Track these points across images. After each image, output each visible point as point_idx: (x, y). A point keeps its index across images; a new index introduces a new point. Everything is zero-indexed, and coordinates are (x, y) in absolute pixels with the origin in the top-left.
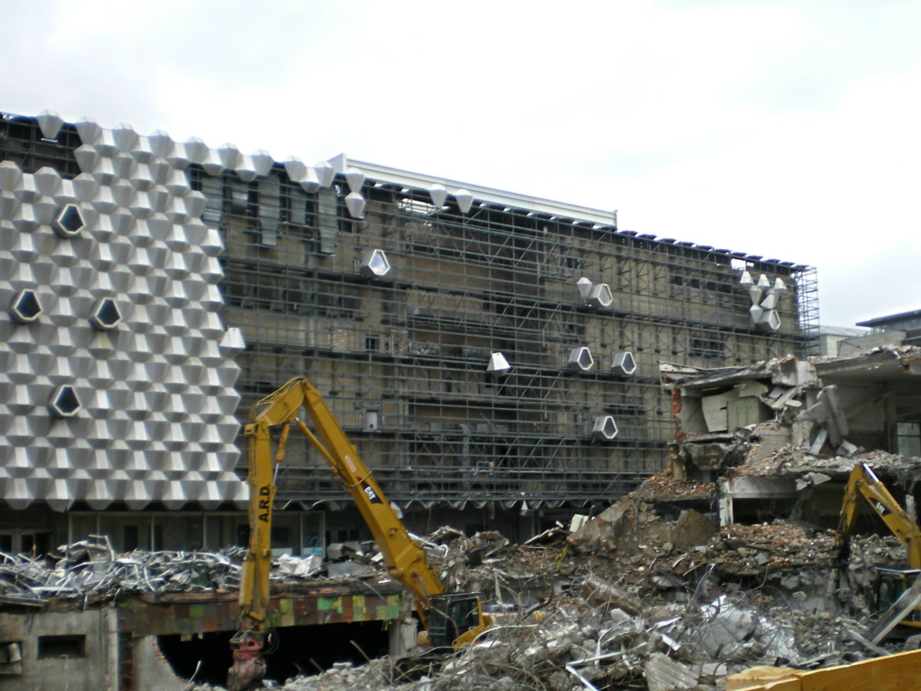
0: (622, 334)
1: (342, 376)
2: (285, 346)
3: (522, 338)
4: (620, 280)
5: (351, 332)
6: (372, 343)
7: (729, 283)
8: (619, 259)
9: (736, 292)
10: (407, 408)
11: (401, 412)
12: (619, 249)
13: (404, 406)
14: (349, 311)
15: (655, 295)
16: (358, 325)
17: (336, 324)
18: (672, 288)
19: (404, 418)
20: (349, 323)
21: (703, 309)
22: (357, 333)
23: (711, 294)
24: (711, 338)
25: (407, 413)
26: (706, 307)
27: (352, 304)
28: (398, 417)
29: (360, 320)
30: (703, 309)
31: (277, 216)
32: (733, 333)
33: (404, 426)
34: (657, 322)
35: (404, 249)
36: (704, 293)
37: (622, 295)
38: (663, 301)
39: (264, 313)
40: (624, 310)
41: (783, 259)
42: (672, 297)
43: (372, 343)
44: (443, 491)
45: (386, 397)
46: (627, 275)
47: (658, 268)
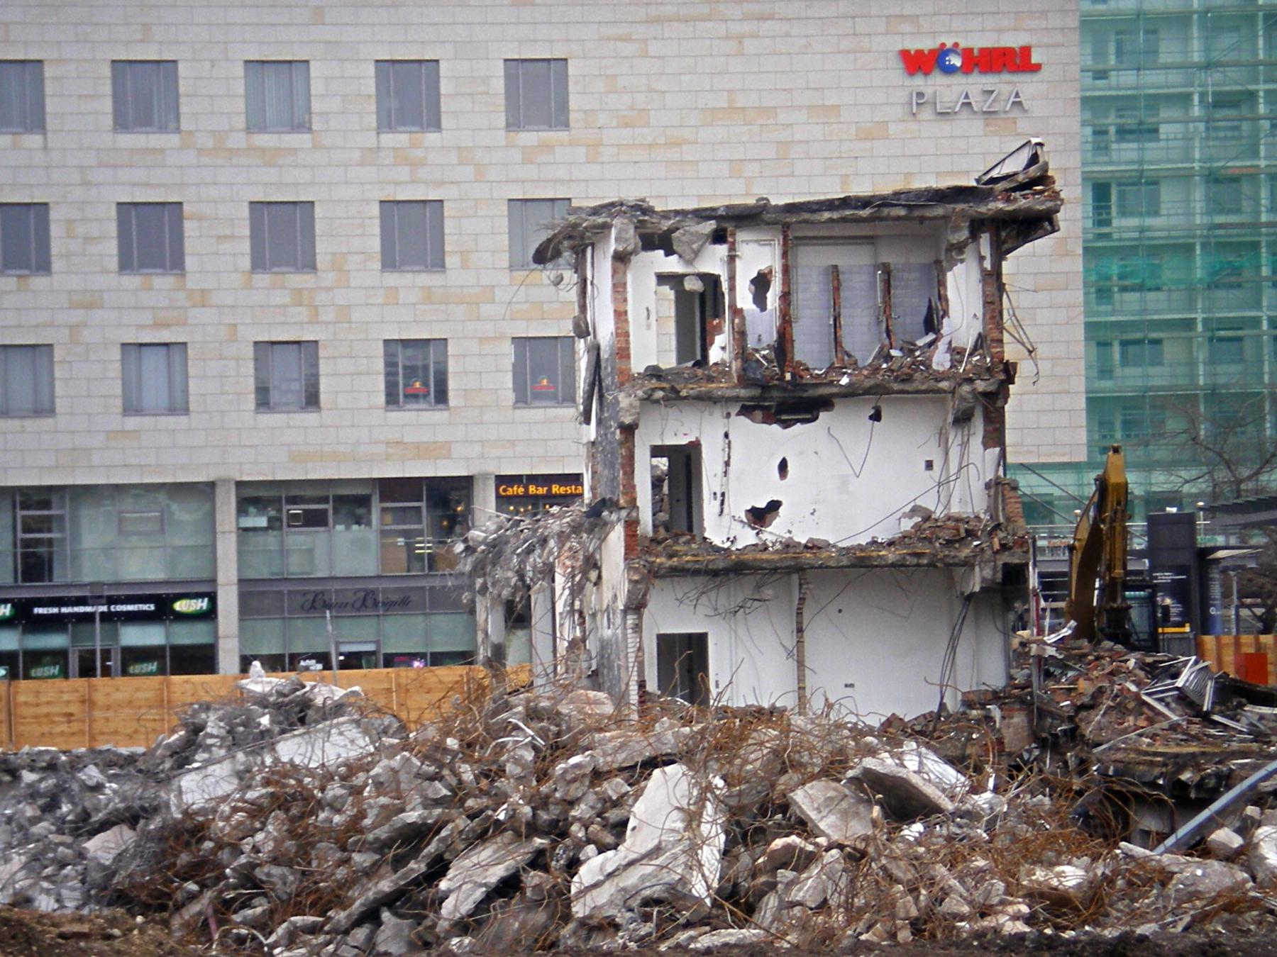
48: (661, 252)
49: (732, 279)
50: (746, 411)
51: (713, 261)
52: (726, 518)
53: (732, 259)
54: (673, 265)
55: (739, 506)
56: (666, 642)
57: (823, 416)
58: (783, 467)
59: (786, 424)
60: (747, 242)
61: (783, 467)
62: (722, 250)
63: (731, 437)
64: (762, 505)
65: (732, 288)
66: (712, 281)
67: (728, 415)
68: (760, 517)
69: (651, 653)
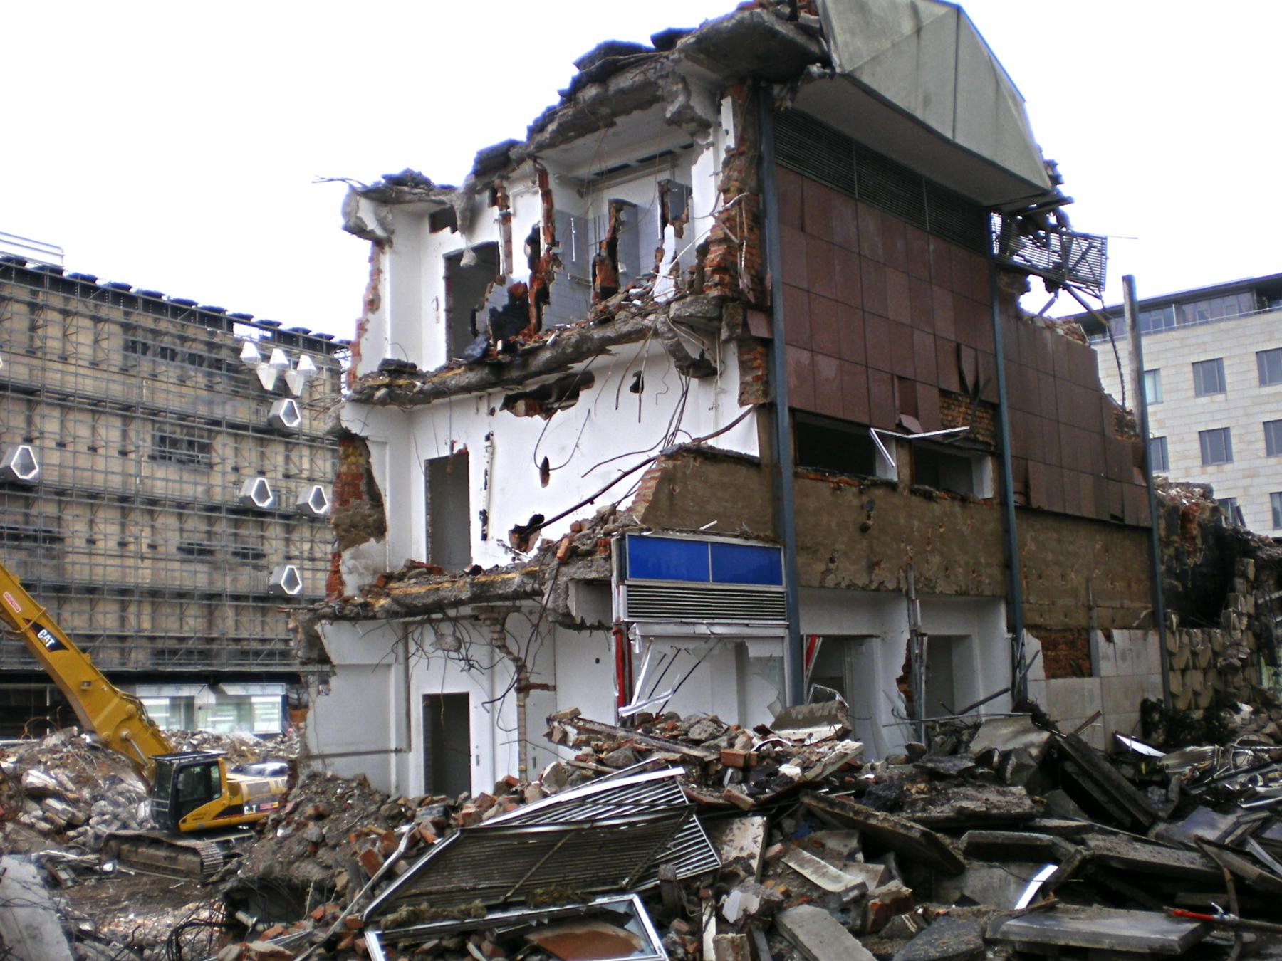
0: (29, 421)
4: (32, 339)
7: (224, 355)
8: (34, 307)
9: (230, 368)
12: (35, 293)
15: (94, 365)
18: (126, 357)
21: (176, 390)
23: (191, 370)
24: (188, 434)
30: (176, 390)
32: (224, 429)
34: (95, 407)
36: (182, 368)
37: (36, 362)
38: (105, 375)
40: (36, 384)
41: (203, 300)
42: (124, 371)
46: (40, 332)
47: (100, 326)
48: (448, 229)
49: (508, 241)
50: (509, 404)
51: (489, 231)
52: (492, 542)
53: (506, 219)
54: (452, 241)
55: (501, 529)
56: (432, 702)
57: (583, 394)
58: (545, 470)
59: (548, 413)
60: (521, 194)
61: (545, 470)
62: (496, 212)
63: (496, 438)
64: (524, 522)
65: (509, 254)
66: (488, 253)
67: (492, 412)
68: (523, 536)
69: (418, 720)
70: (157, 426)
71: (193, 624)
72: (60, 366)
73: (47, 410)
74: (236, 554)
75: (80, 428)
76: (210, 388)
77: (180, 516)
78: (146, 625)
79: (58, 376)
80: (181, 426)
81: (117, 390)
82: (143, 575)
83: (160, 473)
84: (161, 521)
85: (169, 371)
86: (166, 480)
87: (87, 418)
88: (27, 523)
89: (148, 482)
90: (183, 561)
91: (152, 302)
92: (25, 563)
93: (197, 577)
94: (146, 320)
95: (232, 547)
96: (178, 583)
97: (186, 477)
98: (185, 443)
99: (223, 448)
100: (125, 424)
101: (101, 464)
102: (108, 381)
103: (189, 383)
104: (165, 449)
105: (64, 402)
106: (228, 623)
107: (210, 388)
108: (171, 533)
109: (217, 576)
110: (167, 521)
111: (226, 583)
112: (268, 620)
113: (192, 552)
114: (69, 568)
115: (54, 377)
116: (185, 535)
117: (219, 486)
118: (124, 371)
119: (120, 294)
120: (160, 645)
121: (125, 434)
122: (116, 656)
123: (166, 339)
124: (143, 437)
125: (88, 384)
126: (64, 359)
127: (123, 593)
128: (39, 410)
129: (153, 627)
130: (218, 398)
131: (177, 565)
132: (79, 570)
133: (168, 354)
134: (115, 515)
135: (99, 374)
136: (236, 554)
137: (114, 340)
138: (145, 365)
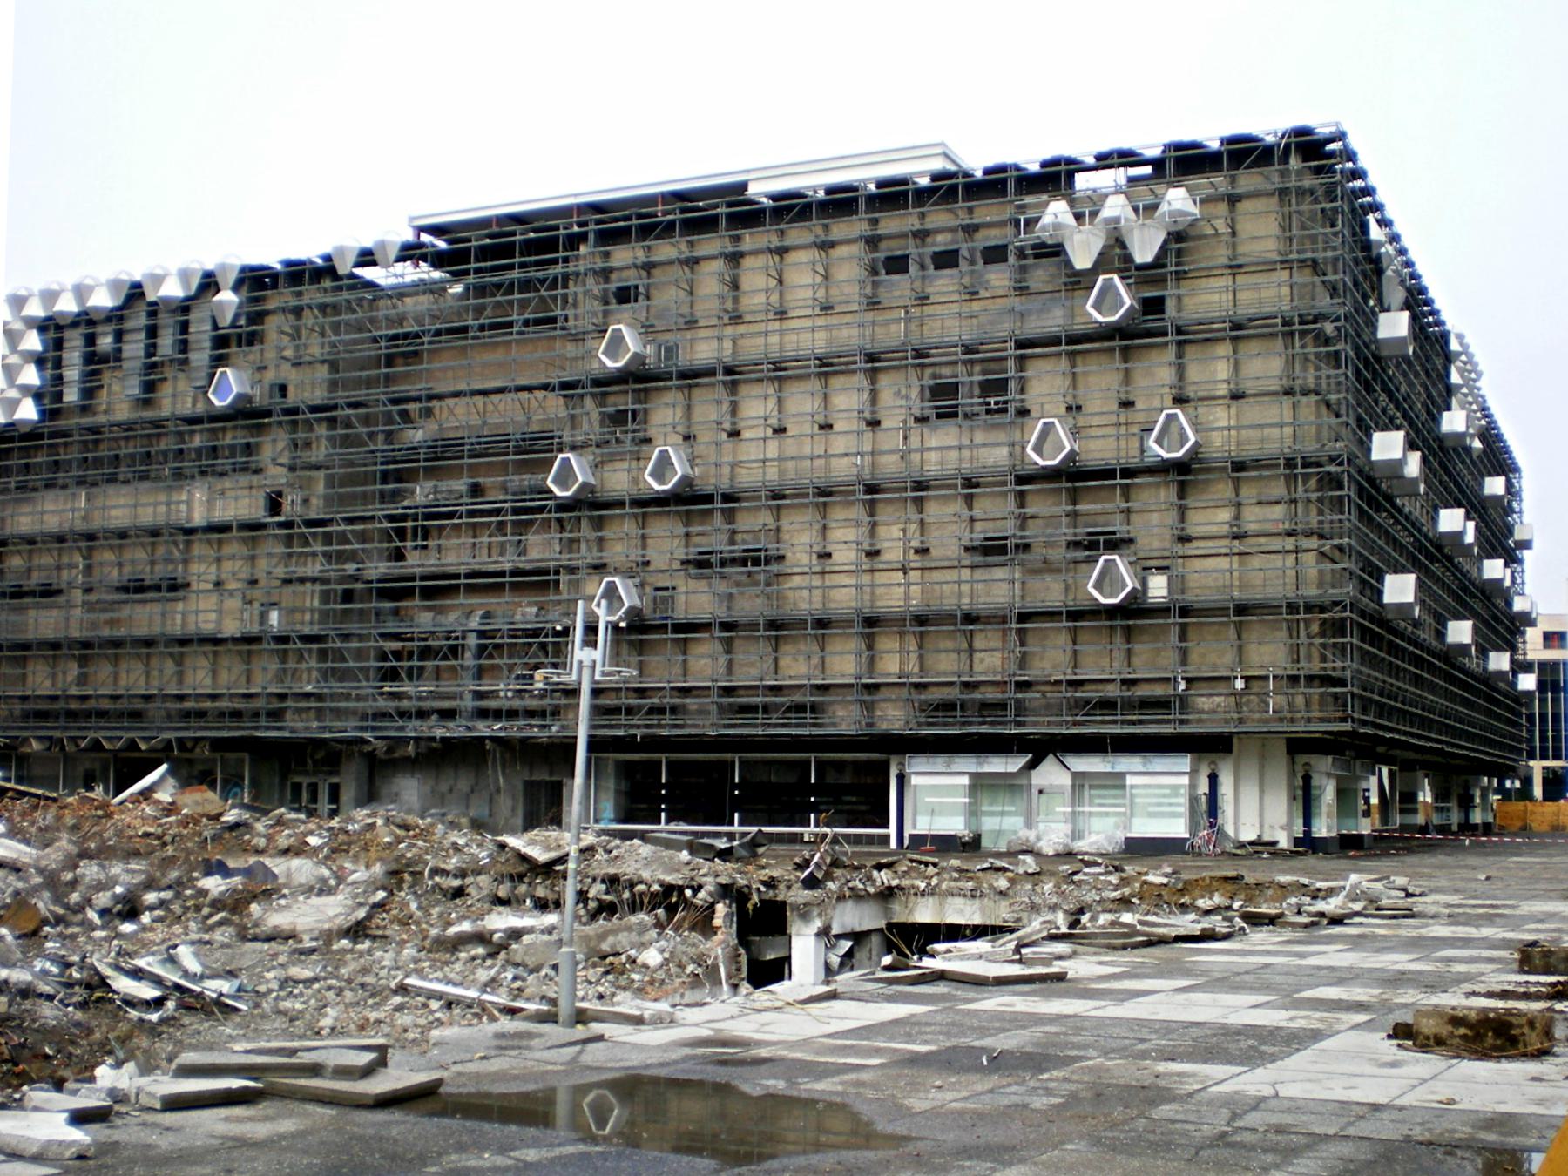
1: (232, 558)
2: (130, 529)
3: (387, 463)
5: (246, 492)
6: (274, 505)
10: (317, 596)
11: (308, 604)
13: (313, 592)
14: (245, 462)
16: (255, 479)
17: (227, 483)
19: (312, 610)
20: (244, 479)
22: (254, 491)
25: (316, 603)
26: (976, 306)
27: (248, 449)
28: (303, 611)
29: (258, 471)
31: (142, 353)
33: (312, 623)
35: (327, 349)
39: (146, 485)
43: (274, 505)
44: (370, 723)
45: (287, 582)
70: (928, 372)
71: (991, 660)
72: (776, 325)
73: (757, 390)
74: (1075, 545)
75: (802, 401)
76: (1022, 290)
77: (969, 499)
78: (913, 666)
79: (760, 341)
80: (972, 362)
81: (848, 335)
82: (894, 595)
83: (933, 441)
84: (933, 510)
85: (945, 284)
86: (943, 450)
87: (815, 385)
88: (732, 542)
89: (916, 457)
90: (973, 567)
91: (893, 194)
92: (731, 595)
93: (998, 588)
94: (893, 223)
95: (1066, 531)
96: (966, 600)
97: (979, 437)
98: (975, 387)
99: (1045, 384)
100: (873, 382)
101: (839, 444)
102: (766, 334)
103: (983, 293)
104: (943, 402)
105: (779, 371)
106: (1052, 657)
107: (1022, 290)
108: (949, 528)
109: (1035, 584)
110: (944, 513)
111: (1051, 593)
112: (1137, 647)
113: (991, 550)
114: (790, 594)
115: (759, 343)
116: (978, 526)
117: (1049, 439)
118: (873, 304)
119: (841, 201)
120: (935, 695)
121: (874, 393)
122: (855, 711)
123: (940, 238)
124: (900, 396)
125: (806, 337)
126: (782, 314)
127: (872, 623)
128: (744, 390)
129: (641, 675)
130: (1034, 303)
131: (966, 574)
132: (802, 597)
133: (946, 260)
134: (858, 512)
135: (834, 320)
136: (1075, 545)
137: (849, 266)
138: (899, 288)
